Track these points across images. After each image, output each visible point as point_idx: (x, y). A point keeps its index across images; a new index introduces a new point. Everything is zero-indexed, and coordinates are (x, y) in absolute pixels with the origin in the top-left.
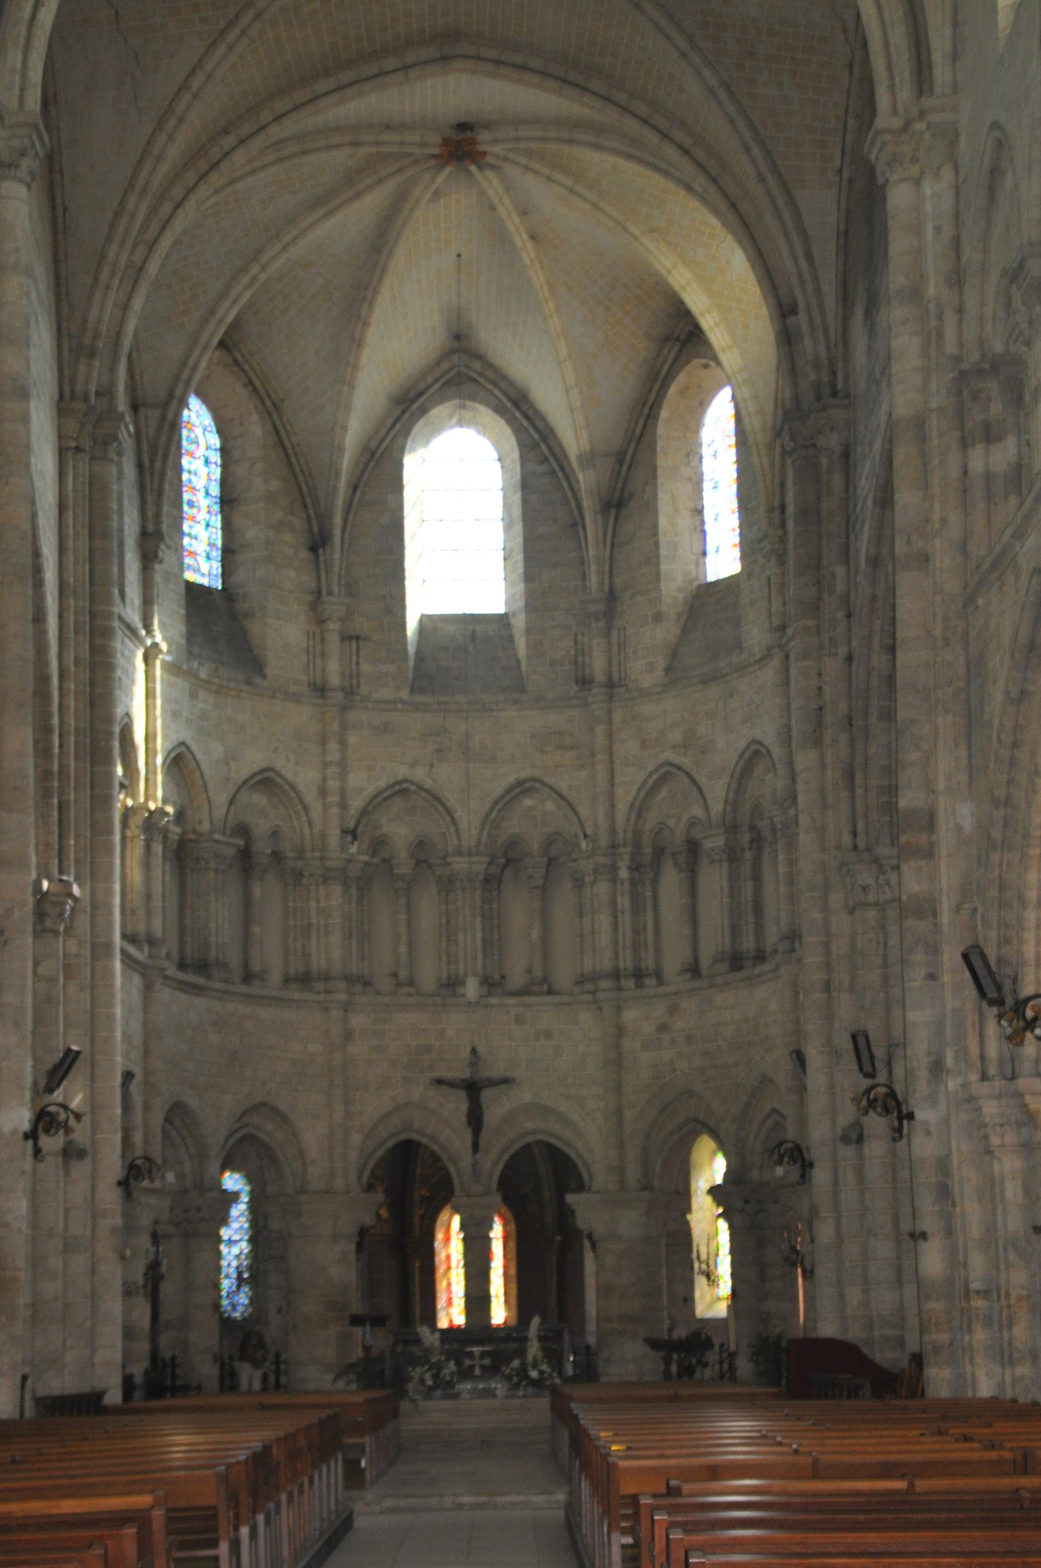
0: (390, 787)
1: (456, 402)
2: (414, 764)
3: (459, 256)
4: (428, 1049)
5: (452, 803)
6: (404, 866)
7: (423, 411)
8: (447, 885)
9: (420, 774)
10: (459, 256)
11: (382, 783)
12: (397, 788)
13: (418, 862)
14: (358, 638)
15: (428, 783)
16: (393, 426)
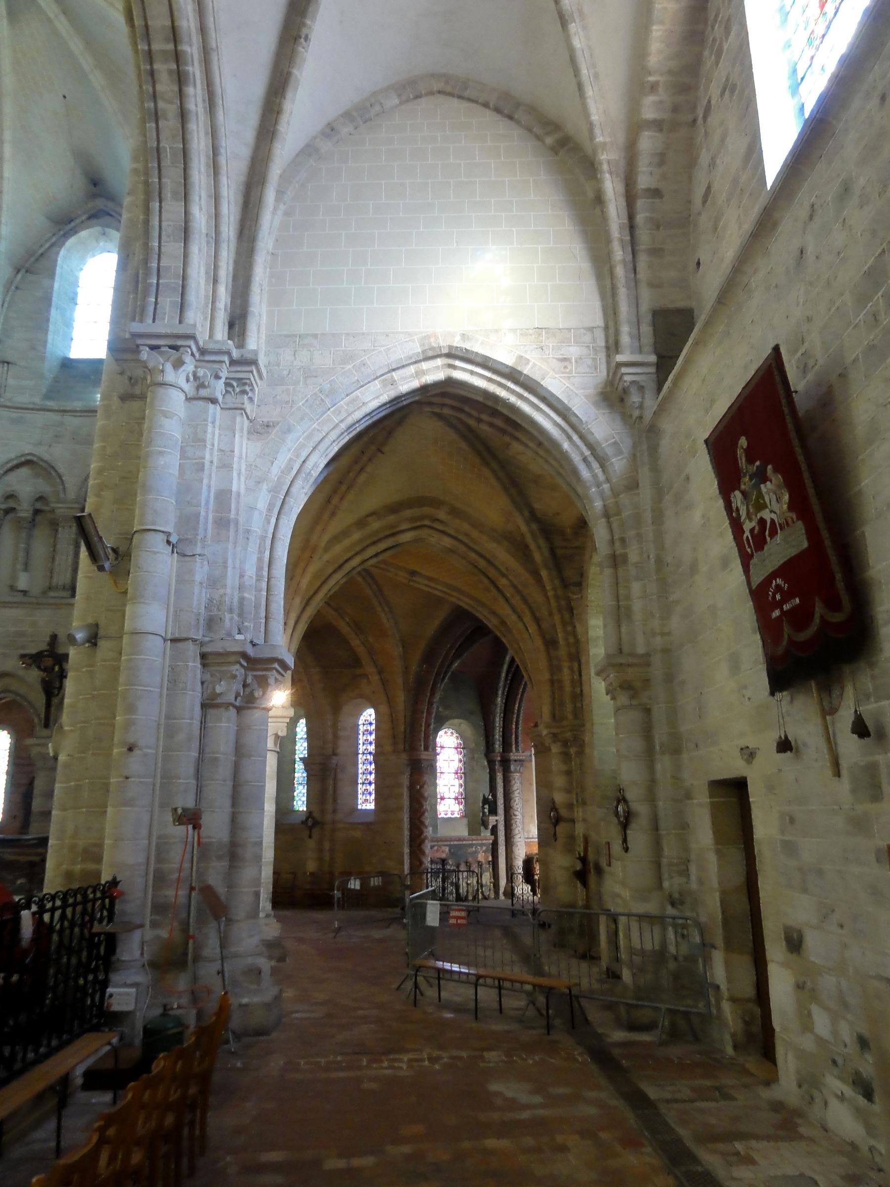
0: (17, 457)
1: (98, 229)
2: (40, 444)
3: (65, 97)
4: (22, 634)
5: (62, 470)
6: (25, 511)
7: (74, 231)
8: (54, 525)
9: (42, 452)
10: (65, 97)
11: (13, 455)
12: (23, 459)
13: (37, 512)
14: (8, 363)
15: (46, 457)
16: (50, 238)
